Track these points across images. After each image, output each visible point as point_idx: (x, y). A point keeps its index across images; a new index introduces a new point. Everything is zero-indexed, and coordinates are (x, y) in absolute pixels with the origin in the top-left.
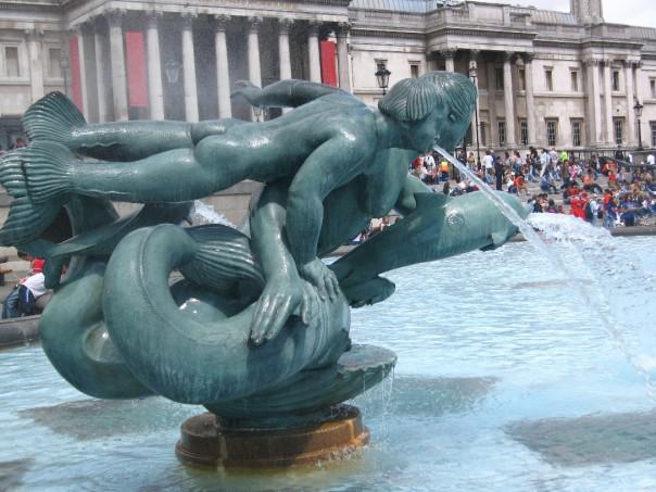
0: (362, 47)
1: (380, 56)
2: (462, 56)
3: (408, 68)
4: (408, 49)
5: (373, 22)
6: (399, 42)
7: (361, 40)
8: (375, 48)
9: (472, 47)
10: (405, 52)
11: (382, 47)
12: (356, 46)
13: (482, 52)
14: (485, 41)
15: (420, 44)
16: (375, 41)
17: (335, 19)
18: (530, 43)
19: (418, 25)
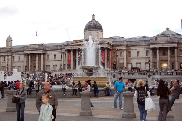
0: (133, 49)
1: (138, 50)
2: (154, 50)
3: (146, 52)
4: (145, 48)
5: (137, 43)
6: (144, 47)
7: (133, 47)
8: (137, 49)
9: (168, 46)
10: (145, 49)
11: (138, 48)
12: (131, 49)
13: (160, 48)
14: (162, 45)
15: (149, 46)
16: (137, 47)
17: (104, 47)
18: (177, 44)
19: (146, 43)
